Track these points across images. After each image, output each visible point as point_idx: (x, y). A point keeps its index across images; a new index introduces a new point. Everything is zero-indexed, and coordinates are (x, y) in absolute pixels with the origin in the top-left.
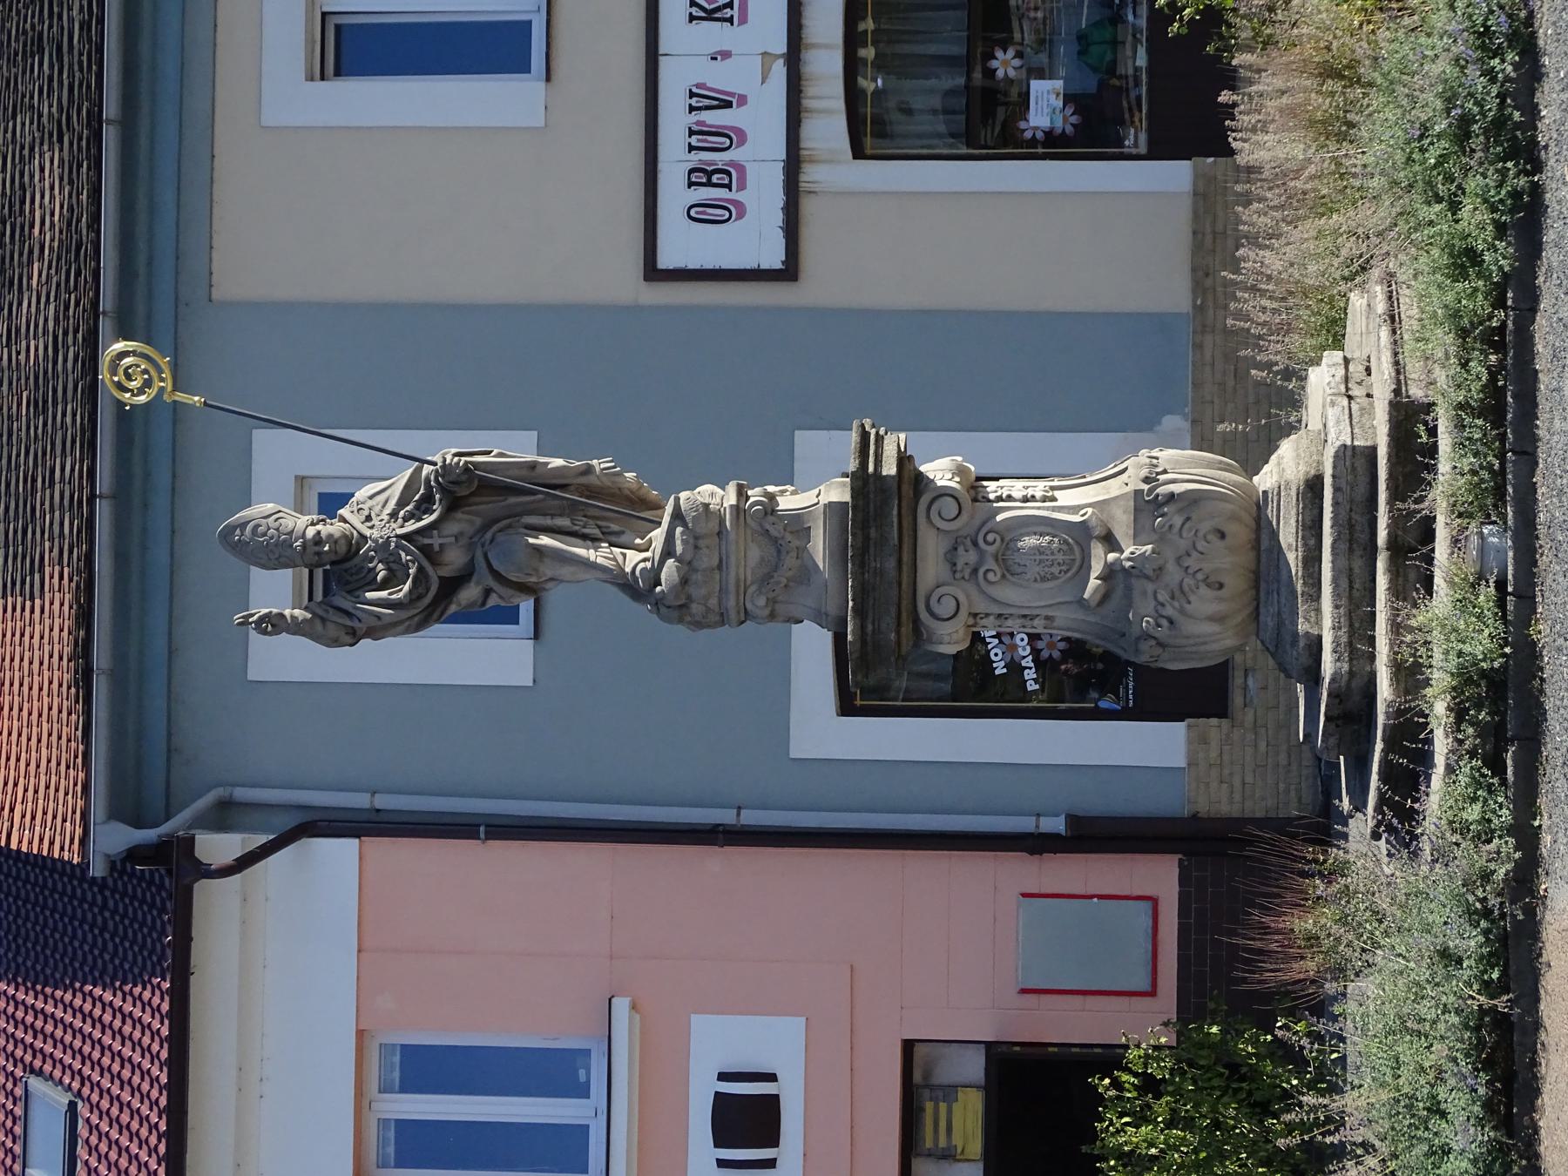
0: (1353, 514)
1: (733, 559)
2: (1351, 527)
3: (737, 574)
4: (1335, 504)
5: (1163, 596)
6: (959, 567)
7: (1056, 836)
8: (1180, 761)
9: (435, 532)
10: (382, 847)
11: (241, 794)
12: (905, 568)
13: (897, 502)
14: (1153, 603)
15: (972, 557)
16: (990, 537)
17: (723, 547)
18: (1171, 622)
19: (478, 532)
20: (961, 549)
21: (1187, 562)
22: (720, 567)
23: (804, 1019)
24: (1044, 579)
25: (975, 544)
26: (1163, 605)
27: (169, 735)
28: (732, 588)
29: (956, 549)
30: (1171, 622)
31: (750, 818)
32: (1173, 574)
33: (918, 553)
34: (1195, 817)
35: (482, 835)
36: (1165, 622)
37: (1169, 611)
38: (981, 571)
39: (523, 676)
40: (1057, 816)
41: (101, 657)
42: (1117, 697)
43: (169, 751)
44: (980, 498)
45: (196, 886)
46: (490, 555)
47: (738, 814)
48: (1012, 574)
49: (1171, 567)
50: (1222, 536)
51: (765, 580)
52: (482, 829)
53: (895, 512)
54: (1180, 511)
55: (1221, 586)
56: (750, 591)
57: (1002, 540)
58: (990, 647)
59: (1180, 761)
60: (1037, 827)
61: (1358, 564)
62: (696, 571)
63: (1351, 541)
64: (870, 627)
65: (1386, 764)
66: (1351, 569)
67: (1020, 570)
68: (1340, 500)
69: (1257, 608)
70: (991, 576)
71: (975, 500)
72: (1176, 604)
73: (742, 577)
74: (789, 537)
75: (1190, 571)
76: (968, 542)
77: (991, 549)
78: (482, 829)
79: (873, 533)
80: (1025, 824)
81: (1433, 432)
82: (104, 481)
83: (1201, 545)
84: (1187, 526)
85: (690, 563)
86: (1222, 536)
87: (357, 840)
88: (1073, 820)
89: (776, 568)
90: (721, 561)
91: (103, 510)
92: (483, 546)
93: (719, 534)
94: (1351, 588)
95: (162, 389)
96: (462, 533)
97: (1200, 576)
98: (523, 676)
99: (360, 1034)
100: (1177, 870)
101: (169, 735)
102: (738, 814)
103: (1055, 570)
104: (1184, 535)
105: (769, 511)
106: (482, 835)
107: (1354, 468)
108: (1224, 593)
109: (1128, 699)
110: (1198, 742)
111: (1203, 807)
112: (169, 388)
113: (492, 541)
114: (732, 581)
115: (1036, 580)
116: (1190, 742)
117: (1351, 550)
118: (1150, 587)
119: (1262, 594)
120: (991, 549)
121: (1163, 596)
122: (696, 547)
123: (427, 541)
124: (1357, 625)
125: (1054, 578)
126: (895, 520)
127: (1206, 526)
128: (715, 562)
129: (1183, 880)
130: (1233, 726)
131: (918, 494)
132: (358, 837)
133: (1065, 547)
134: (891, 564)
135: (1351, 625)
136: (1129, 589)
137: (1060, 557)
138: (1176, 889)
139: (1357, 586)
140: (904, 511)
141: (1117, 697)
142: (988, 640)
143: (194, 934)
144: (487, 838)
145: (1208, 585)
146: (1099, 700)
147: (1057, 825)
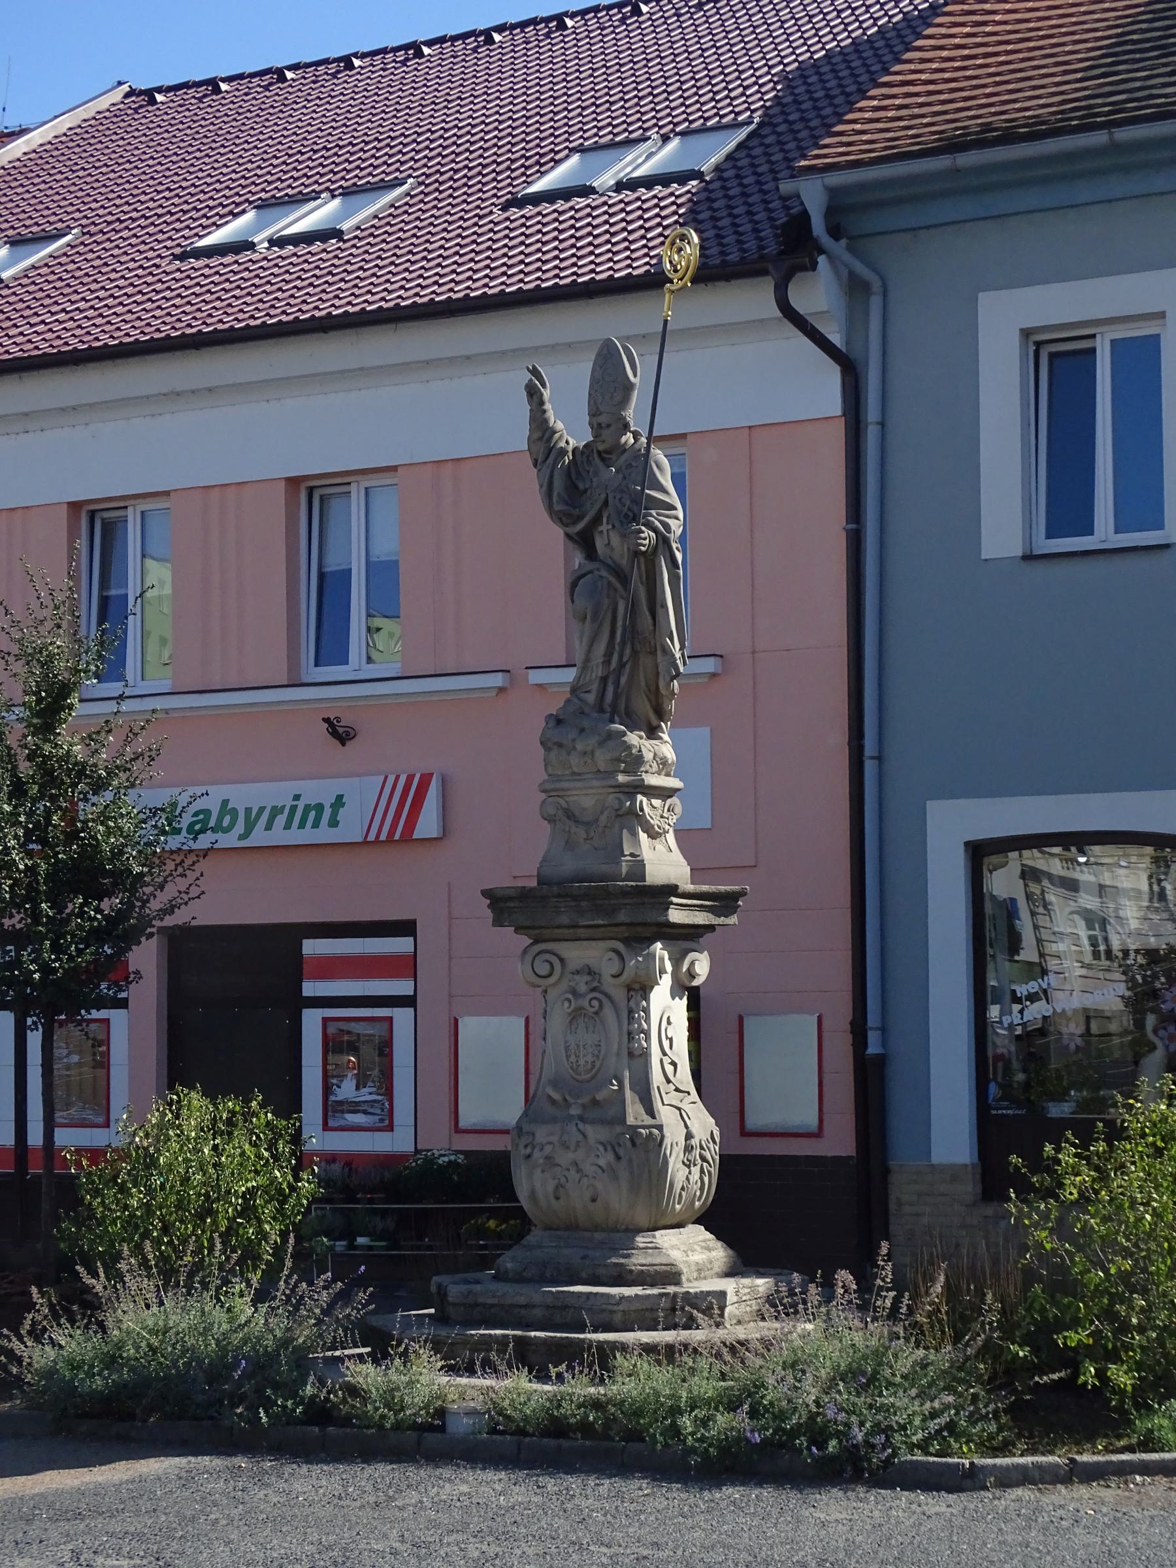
0: (572, 1310)
1: (578, 784)
2: (565, 1307)
3: (575, 789)
4: (580, 1294)
5: (548, 1149)
6: (577, 977)
7: (866, 1047)
8: (936, 1159)
9: (610, 527)
10: (837, 435)
11: (876, 302)
12: (571, 931)
13: (606, 922)
14: (544, 1141)
15: (582, 988)
16: (595, 1003)
17: (589, 776)
18: (529, 1156)
19: (614, 562)
20: (587, 978)
21: (573, 1172)
22: (574, 773)
23: (709, 826)
24: (567, 1049)
25: (594, 990)
26: (541, 1150)
27: (928, 227)
28: (559, 785)
29: (589, 974)
30: (529, 1156)
31: (870, 767)
32: (565, 1158)
33: (585, 943)
34: (886, 1171)
35: (850, 526)
36: (528, 1151)
37: (537, 1154)
38: (570, 996)
39: (988, 551)
40: (884, 1044)
41: (966, 159)
42: (1001, 1099)
43: (914, 229)
44: (632, 993)
45: (769, 278)
46: (589, 576)
47: (872, 758)
48: (571, 1022)
49: (571, 1156)
50: (594, 1200)
51: (569, 814)
52: (854, 526)
53: (601, 922)
54: (609, 1164)
55: (557, 1198)
56: (561, 801)
57: (596, 1013)
58: (1040, 980)
59: (936, 1159)
60: (871, 1029)
61: (538, 1312)
62: (569, 754)
63: (554, 1307)
64: (511, 904)
65: (507, 1336)
66: (534, 1306)
67: (573, 1028)
68: (582, 1300)
69: (550, 1229)
70: (566, 1004)
71: (629, 989)
72: (541, 1161)
73: (569, 793)
74: (600, 829)
75: (566, 1173)
76: (595, 984)
77: (585, 1003)
78: (854, 526)
79: (584, 904)
80: (873, 1020)
81: (560, 1377)
82: (1124, 134)
83: (585, 1181)
84: (600, 1171)
85: (574, 748)
86: (594, 1200)
87: (839, 413)
88: (881, 1061)
89: (576, 822)
90: (580, 774)
91: (1099, 138)
92: (598, 569)
93: (599, 771)
94: (521, 1306)
95: (671, 282)
96: (612, 549)
97: (563, 1180)
98: (988, 551)
99: (683, 436)
100: (843, 1154)
101: (928, 227)
102: (872, 758)
103: (573, 1058)
104: (594, 1168)
105: (620, 813)
106: (850, 526)
107: (603, 1311)
108: (553, 1201)
109: (997, 1109)
110: (953, 1173)
111: (895, 1179)
112: (674, 288)
113: (601, 577)
114: (566, 785)
115: (566, 1042)
116: (952, 1166)
117: (548, 1307)
118: (555, 1139)
119: (559, 1233)
120: (585, 1003)
121: (548, 1149)
122: (585, 753)
123: (605, 520)
124: (493, 1310)
125: (568, 1057)
126: (595, 922)
127: (599, 1186)
128: (576, 770)
129: (837, 1160)
130: (967, 1206)
131: (626, 941)
132: (844, 415)
133: (589, 1066)
134: (565, 919)
135: (492, 1306)
136: (554, 1120)
137: (582, 1062)
138: (829, 1155)
139: (523, 1312)
140: (602, 929)
141: (1001, 1099)
142: (1046, 978)
143: (733, 282)
144: (847, 531)
145: (557, 1187)
146: (997, 1082)
147: (873, 1048)
